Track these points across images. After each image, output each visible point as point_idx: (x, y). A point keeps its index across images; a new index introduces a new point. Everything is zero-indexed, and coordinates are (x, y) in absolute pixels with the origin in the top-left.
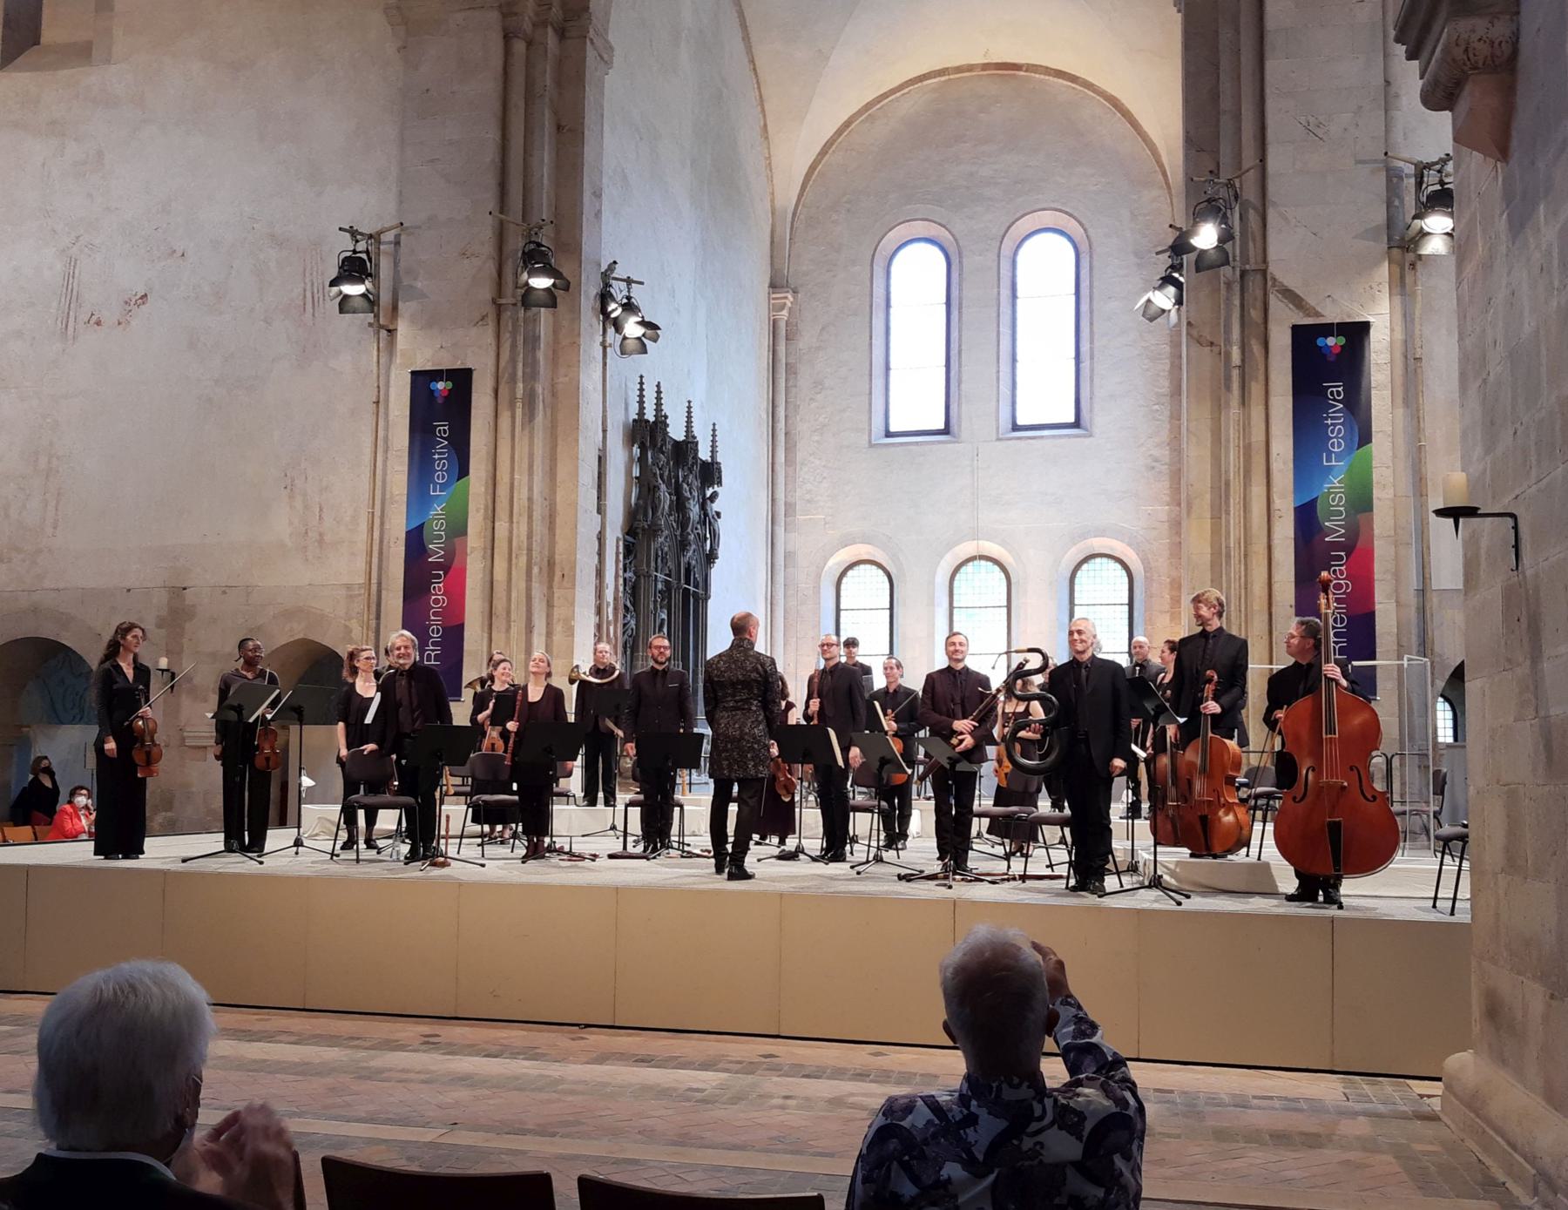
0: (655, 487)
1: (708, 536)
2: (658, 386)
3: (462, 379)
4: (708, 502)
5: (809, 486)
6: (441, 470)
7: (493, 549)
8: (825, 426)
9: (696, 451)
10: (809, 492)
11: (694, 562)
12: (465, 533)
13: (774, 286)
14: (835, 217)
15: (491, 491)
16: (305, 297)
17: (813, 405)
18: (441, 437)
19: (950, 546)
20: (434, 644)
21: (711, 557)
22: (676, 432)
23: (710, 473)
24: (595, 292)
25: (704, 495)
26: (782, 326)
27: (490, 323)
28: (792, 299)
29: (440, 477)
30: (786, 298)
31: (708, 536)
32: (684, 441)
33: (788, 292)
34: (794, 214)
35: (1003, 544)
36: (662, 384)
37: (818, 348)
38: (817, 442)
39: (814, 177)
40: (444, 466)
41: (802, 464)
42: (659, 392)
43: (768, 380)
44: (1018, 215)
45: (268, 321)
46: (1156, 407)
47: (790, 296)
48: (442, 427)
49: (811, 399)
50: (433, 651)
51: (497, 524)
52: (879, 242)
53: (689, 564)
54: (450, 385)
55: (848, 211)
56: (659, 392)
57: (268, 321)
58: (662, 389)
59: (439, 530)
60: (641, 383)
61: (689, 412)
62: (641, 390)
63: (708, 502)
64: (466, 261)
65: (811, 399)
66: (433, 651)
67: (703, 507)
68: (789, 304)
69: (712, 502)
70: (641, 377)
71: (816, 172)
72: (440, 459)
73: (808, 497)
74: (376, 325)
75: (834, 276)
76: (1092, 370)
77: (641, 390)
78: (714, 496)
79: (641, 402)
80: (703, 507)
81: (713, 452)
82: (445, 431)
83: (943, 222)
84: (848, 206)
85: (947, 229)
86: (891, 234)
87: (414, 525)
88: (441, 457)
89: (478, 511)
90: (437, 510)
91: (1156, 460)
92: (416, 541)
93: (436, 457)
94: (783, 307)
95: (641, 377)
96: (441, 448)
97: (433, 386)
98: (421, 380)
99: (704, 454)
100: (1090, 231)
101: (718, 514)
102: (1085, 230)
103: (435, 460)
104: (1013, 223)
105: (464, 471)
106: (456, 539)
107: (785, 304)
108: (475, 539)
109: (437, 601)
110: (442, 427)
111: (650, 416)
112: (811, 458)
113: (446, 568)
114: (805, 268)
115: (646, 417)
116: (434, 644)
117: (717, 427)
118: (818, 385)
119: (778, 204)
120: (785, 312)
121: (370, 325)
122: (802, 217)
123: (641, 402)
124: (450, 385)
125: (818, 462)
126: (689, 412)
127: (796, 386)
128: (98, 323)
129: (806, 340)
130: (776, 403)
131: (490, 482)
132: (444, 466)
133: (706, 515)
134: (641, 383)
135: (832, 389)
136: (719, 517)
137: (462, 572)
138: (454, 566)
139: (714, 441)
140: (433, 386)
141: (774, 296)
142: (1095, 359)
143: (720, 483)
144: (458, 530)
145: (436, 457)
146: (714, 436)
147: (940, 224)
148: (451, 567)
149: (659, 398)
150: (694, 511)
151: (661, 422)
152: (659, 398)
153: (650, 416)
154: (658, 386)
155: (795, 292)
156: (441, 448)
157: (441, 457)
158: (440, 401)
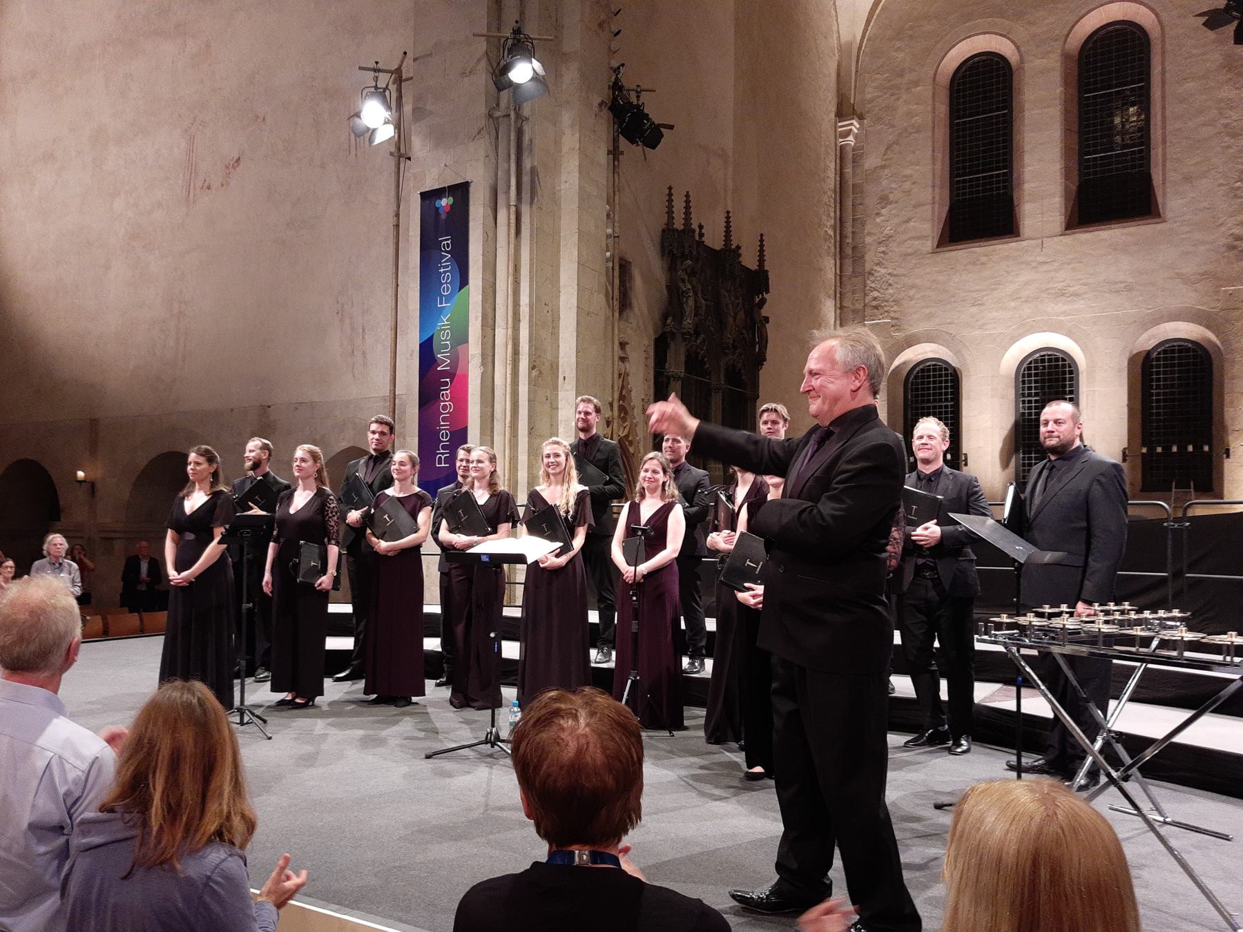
0: (683, 292)
2: (687, 196)
5: (876, 294)
6: (446, 283)
7: (494, 356)
8: (891, 237)
10: (875, 299)
11: (739, 365)
12: (467, 342)
13: (840, 115)
14: (898, 44)
15: (490, 301)
16: (350, 140)
17: (878, 220)
19: (1014, 340)
20: (443, 447)
21: (760, 359)
22: (714, 239)
23: (758, 281)
24: (600, 100)
25: (753, 300)
26: (849, 149)
27: (487, 136)
28: (858, 126)
29: (446, 289)
30: (852, 124)
32: (721, 250)
33: (853, 119)
34: (860, 48)
35: (1069, 334)
37: (883, 167)
38: (883, 252)
39: (877, 12)
40: (448, 279)
41: (870, 273)
42: (688, 202)
43: (835, 202)
44: (1083, 11)
45: (323, 166)
47: (855, 122)
48: (446, 241)
49: (878, 214)
50: (442, 454)
52: (941, 61)
54: (451, 200)
55: (911, 36)
56: (688, 202)
57: (323, 166)
59: (446, 340)
60: (670, 195)
62: (670, 201)
64: (466, 79)
65: (877, 214)
66: (442, 454)
70: (670, 188)
71: (879, 8)
72: (445, 272)
73: (874, 303)
74: (396, 154)
75: (899, 99)
76: (1164, 155)
78: (763, 301)
79: (670, 213)
81: (761, 261)
84: (910, 33)
85: (1009, 39)
86: (952, 51)
87: (426, 337)
88: (446, 268)
89: (476, 318)
90: (444, 320)
92: (427, 350)
93: (442, 270)
94: (849, 133)
95: (670, 188)
96: (445, 262)
97: (437, 204)
98: (428, 197)
100: (1164, 16)
101: (767, 319)
102: (1157, 15)
103: (441, 273)
104: (1079, 21)
105: (464, 282)
106: (459, 347)
107: (851, 130)
108: (474, 348)
109: (445, 407)
110: (446, 241)
111: (679, 224)
112: (878, 268)
113: (451, 375)
114: (870, 96)
115: (675, 226)
116: (443, 447)
117: (764, 238)
118: (884, 200)
119: (843, 41)
120: (851, 138)
121: (392, 154)
122: (867, 50)
123: (670, 213)
124: (451, 200)
125: (883, 271)
127: (861, 204)
128: (209, 188)
129: (871, 162)
130: (843, 220)
131: (490, 291)
132: (448, 279)
135: (896, 202)
136: (768, 322)
137: (466, 377)
138: (458, 373)
139: (761, 251)
140: (437, 204)
141: (840, 124)
142: (1168, 144)
143: (767, 292)
144: (461, 338)
145: (442, 270)
146: (762, 246)
147: (1001, 35)
148: (456, 377)
149: (688, 207)
152: (688, 207)
153: (679, 224)
154: (687, 196)
155: (861, 118)
156: (445, 262)
157: (446, 268)
158: (443, 216)
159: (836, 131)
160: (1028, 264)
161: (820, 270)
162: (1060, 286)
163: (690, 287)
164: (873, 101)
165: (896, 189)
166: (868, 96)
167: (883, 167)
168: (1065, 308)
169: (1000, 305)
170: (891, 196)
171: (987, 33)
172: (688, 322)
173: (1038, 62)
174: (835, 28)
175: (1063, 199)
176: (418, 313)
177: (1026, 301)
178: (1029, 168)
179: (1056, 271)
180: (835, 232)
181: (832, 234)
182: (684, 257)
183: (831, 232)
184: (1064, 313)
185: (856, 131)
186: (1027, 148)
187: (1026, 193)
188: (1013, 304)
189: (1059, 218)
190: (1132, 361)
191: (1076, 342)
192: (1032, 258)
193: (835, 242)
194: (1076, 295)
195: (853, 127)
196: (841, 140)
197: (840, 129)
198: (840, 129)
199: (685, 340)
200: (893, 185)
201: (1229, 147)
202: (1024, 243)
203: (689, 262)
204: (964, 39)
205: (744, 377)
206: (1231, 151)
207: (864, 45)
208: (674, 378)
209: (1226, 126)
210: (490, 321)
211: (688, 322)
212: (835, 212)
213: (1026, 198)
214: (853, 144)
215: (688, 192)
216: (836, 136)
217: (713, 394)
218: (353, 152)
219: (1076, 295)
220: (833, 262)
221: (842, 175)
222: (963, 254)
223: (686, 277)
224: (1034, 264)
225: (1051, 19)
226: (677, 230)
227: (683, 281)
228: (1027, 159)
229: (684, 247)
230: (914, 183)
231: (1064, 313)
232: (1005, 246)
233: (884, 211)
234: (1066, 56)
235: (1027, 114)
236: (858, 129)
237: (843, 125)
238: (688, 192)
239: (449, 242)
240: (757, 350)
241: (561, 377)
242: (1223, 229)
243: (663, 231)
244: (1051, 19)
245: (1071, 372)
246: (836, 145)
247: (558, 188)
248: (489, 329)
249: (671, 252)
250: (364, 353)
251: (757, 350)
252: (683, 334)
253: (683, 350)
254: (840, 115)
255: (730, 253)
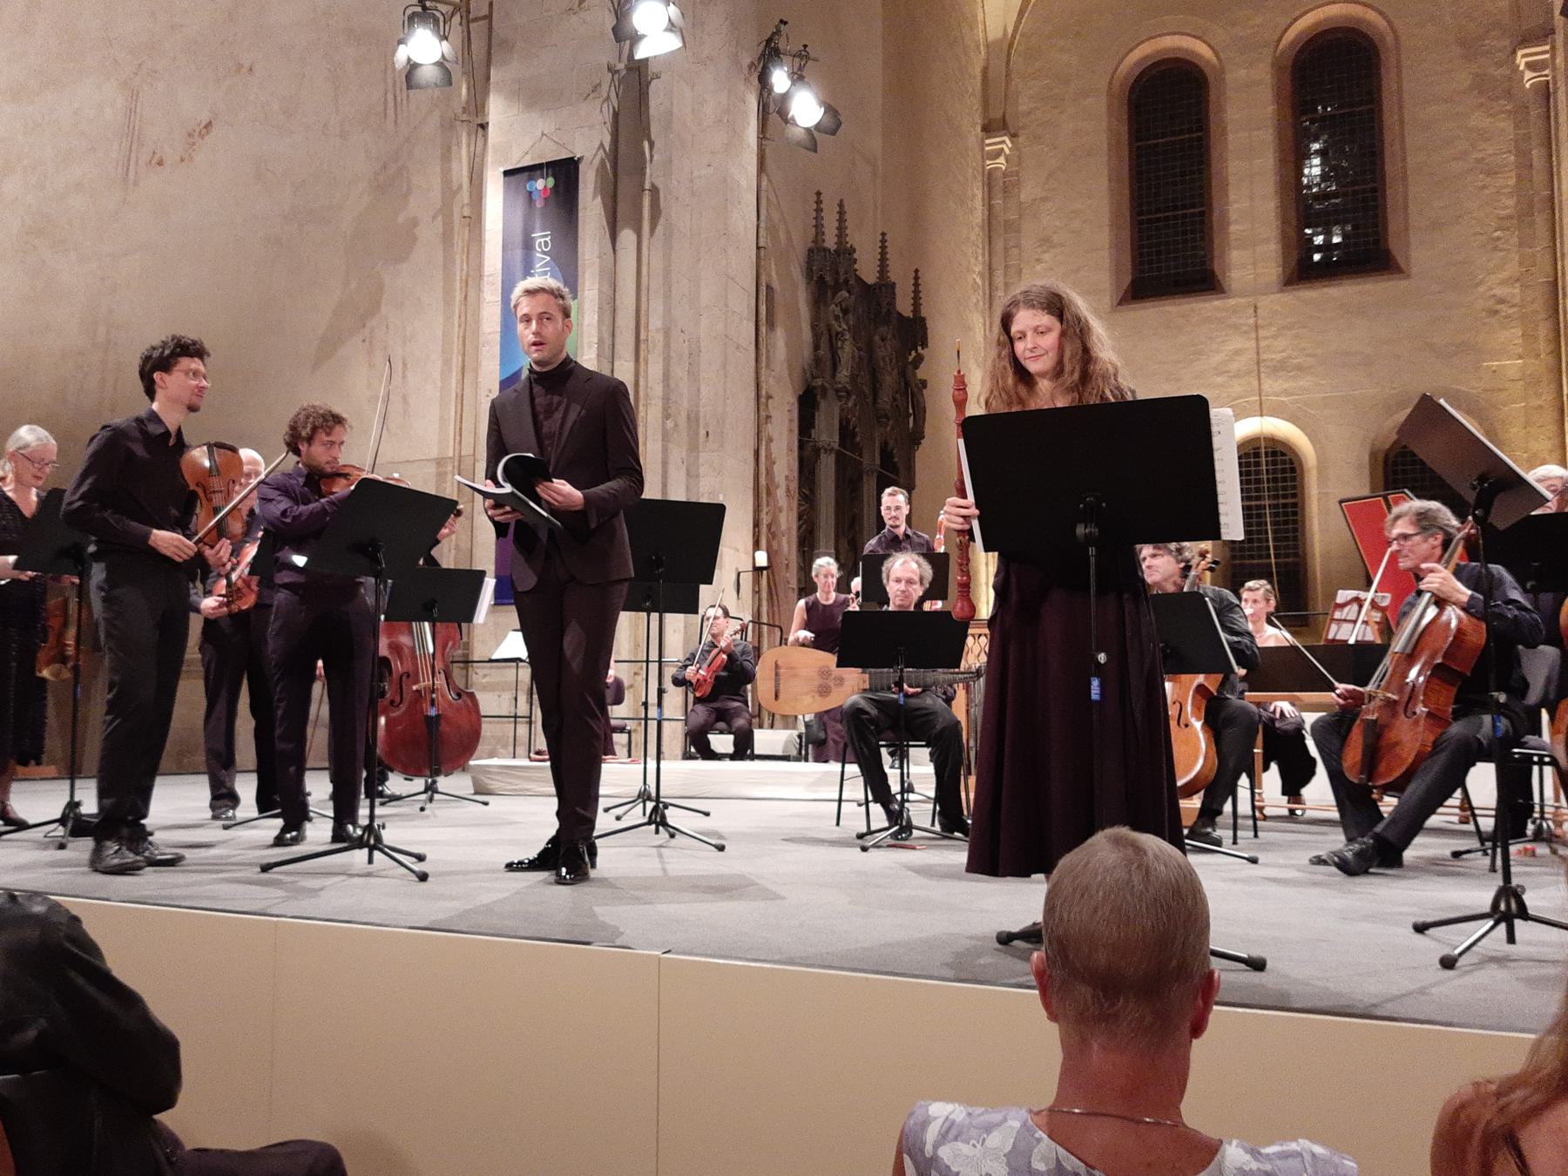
0: (837, 334)
1: (911, 411)
2: (841, 205)
3: (565, 172)
4: (910, 367)
9: (892, 303)
17: (1039, 267)
18: (544, 253)
22: (868, 271)
28: (1010, 145)
30: (1003, 142)
31: (911, 411)
33: (1005, 135)
34: (1011, 46)
36: (846, 203)
37: (1044, 199)
42: (841, 213)
44: (1297, 13)
46: (1498, 234)
47: (1006, 139)
49: (1038, 260)
51: (616, 364)
53: (886, 443)
55: (1078, 33)
56: (841, 213)
58: (846, 208)
60: (819, 202)
61: (883, 247)
62: (819, 210)
63: (910, 367)
67: (903, 374)
68: (1007, 151)
69: (916, 367)
77: (819, 210)
78: (919, 359)
79: (819, 227)
80: (903, 374)
82: (546, 242)
83: (1200, 34)
91: (1502, 301)
94: (999, 153)
99: (904, 306)
101: (924, 384)
107: (1002, 149)
111: (830, 242)
115: (825, 245)
120: (1002, 160)
123: (819, 227)
126: (883, 247)
129: (1028, 191)
133: (907, 384)
134: (819, 202)
135: (1062, 245)
141: (987, 141)
143: (924, 344)
147: (1194, 37)
149: (841, 220)
150: (889, 380)
151: (845, 252)
152: (841, 220)
153: (830, 242)
154: (841, 205)
155: (1013, 136)
159: (983, 149)
160: (1236, 327)
161: (970, 329)
162: (1278, 356)
163: (845, 327)
164: (1029, 113)
165: (1062, 228)
166: (1023, 108)
167: (1044, 199)
168: (1286, 386)
169: (1202, 381)
170: (1055, 237)
171: (1175, 34)
172: (844, 374)
173: (1243, 72)
174: (980, 18)
175: (1280, 246)
176: (498, 337)
177: (1235, 376)
178: (1236, 206)
179: (1275, 337)
180: (984, 282)
181: (980, 283)
182: (836, 288)
183: (979, 281)
184: (1286, 392)
185: (1007, 151)
186: (1232, 180)
187: (1232, 237)
188: (1219, 380)
189: (1274, 271)
190: (1373, 455)
191: (1302, 430)
192: (1241, 321)
193: (984, 294)
194: (1299, 368)
195: (1004, 146)
196: (988, 162)
197: (987, 148)
198: (987, 148)
199: (840, 398)
200: (1057, 224)
201: (1484, 187)
202: (1232, 302)
203: (844, 294)
204: (1147, 40)
205: (896, 460)
206: (1487, 191)
207: (1016, 42)
208: (826, 450)
209: (1478, 161)
210: (608, 352)
211: (844, 374)
212: (983, 255)
213: (1233, 243)
214: (1004, 168)
215: (841, 201)
216: (983, 156)
217: (865, 477)
218: (391, 112)
219: (1299, 368)
220: (981, 320)
221: (990, 208)
222: (1152, 313)
223: (841, 315)
224: (1244, 328)
225: (1258, 20)
226: (826, 250)
227: (837, 318)
228: (1232, 196)
229: (837, 273)
230: (1085, 221)
231: (1286, 392)
232: (1207, 305)
233: (1046, 257)
234: (1277, 67)
235: (1231, 137)
236: (1010, 149)
237: (992, 143)
238: (841, 201)
239: (548, 239)
240: (911, 425)
241: (702, 432)
242: (1481, 289)
243: (810, 251)
244: (1258, 20)
245: (1293, 470)
246: (983, 168)
247: (696, 173)
248: (606, 361)
249: (821, 278)
250: (405, 399)
251: (911, 425)
252: (837, 391)
253: (837, 411)
254: (988, 129)
255: (885, 287)
